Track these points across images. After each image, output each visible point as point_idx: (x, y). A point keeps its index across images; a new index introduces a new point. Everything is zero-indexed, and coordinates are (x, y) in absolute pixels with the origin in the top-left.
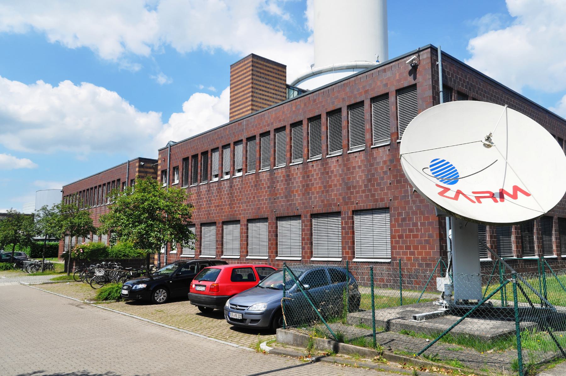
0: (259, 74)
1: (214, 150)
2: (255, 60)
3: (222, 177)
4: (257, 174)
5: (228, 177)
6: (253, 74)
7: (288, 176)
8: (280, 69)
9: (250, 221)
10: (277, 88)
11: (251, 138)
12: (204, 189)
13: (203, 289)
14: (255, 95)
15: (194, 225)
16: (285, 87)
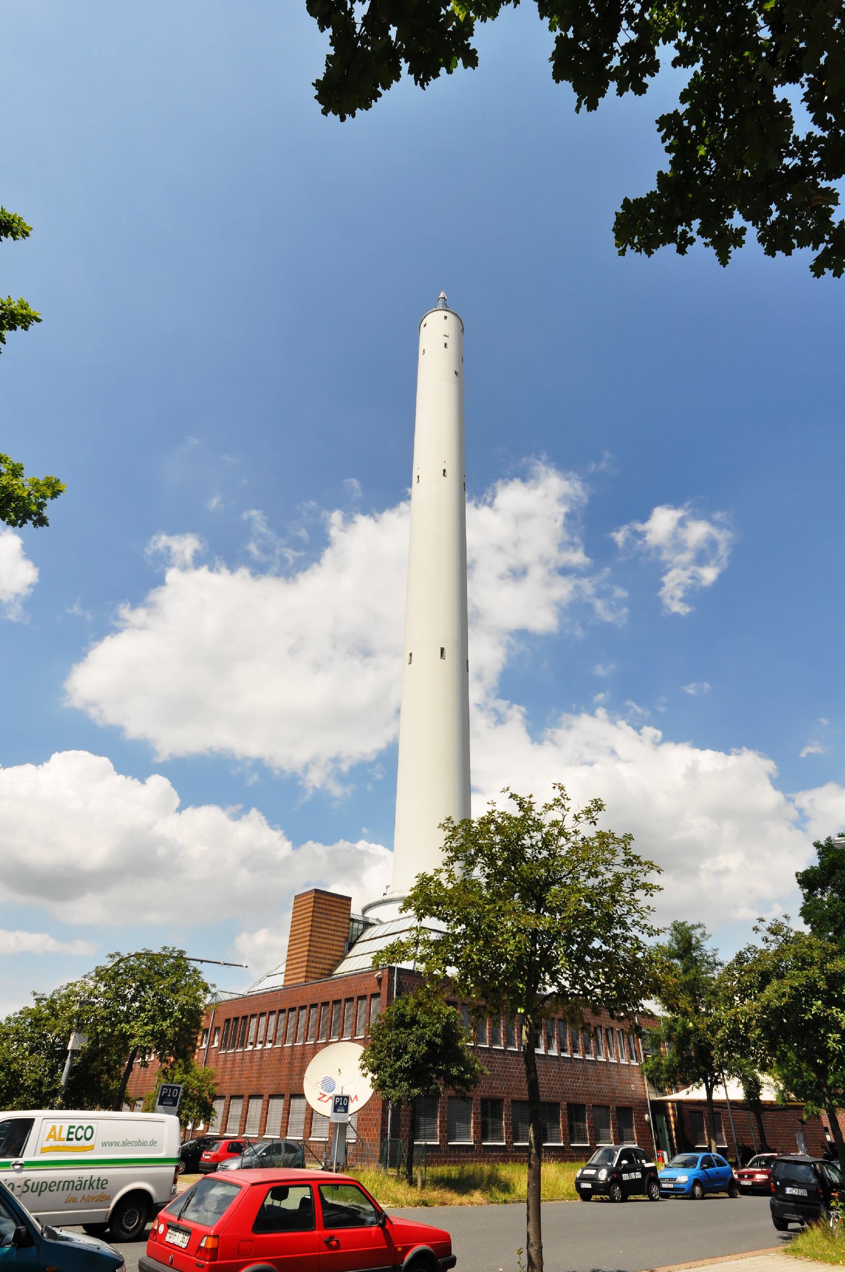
0: (320, 910)
1: (253, 1016)
2: (318, 895)
3: (255, 1046)
4: (282, 1048)
5: (259, 1047)
6: (313, 911)
7: (303, 1054)
8: (344, 901)
9: (272, 1096)
10: (339, 924)
11: (282, 1011)
12: (238, 1057)
13: (208, 1157)
14: (314, 934)
15: (222, 1097)
16: (348, 921)
